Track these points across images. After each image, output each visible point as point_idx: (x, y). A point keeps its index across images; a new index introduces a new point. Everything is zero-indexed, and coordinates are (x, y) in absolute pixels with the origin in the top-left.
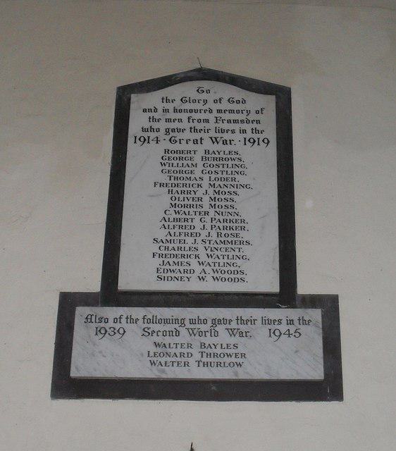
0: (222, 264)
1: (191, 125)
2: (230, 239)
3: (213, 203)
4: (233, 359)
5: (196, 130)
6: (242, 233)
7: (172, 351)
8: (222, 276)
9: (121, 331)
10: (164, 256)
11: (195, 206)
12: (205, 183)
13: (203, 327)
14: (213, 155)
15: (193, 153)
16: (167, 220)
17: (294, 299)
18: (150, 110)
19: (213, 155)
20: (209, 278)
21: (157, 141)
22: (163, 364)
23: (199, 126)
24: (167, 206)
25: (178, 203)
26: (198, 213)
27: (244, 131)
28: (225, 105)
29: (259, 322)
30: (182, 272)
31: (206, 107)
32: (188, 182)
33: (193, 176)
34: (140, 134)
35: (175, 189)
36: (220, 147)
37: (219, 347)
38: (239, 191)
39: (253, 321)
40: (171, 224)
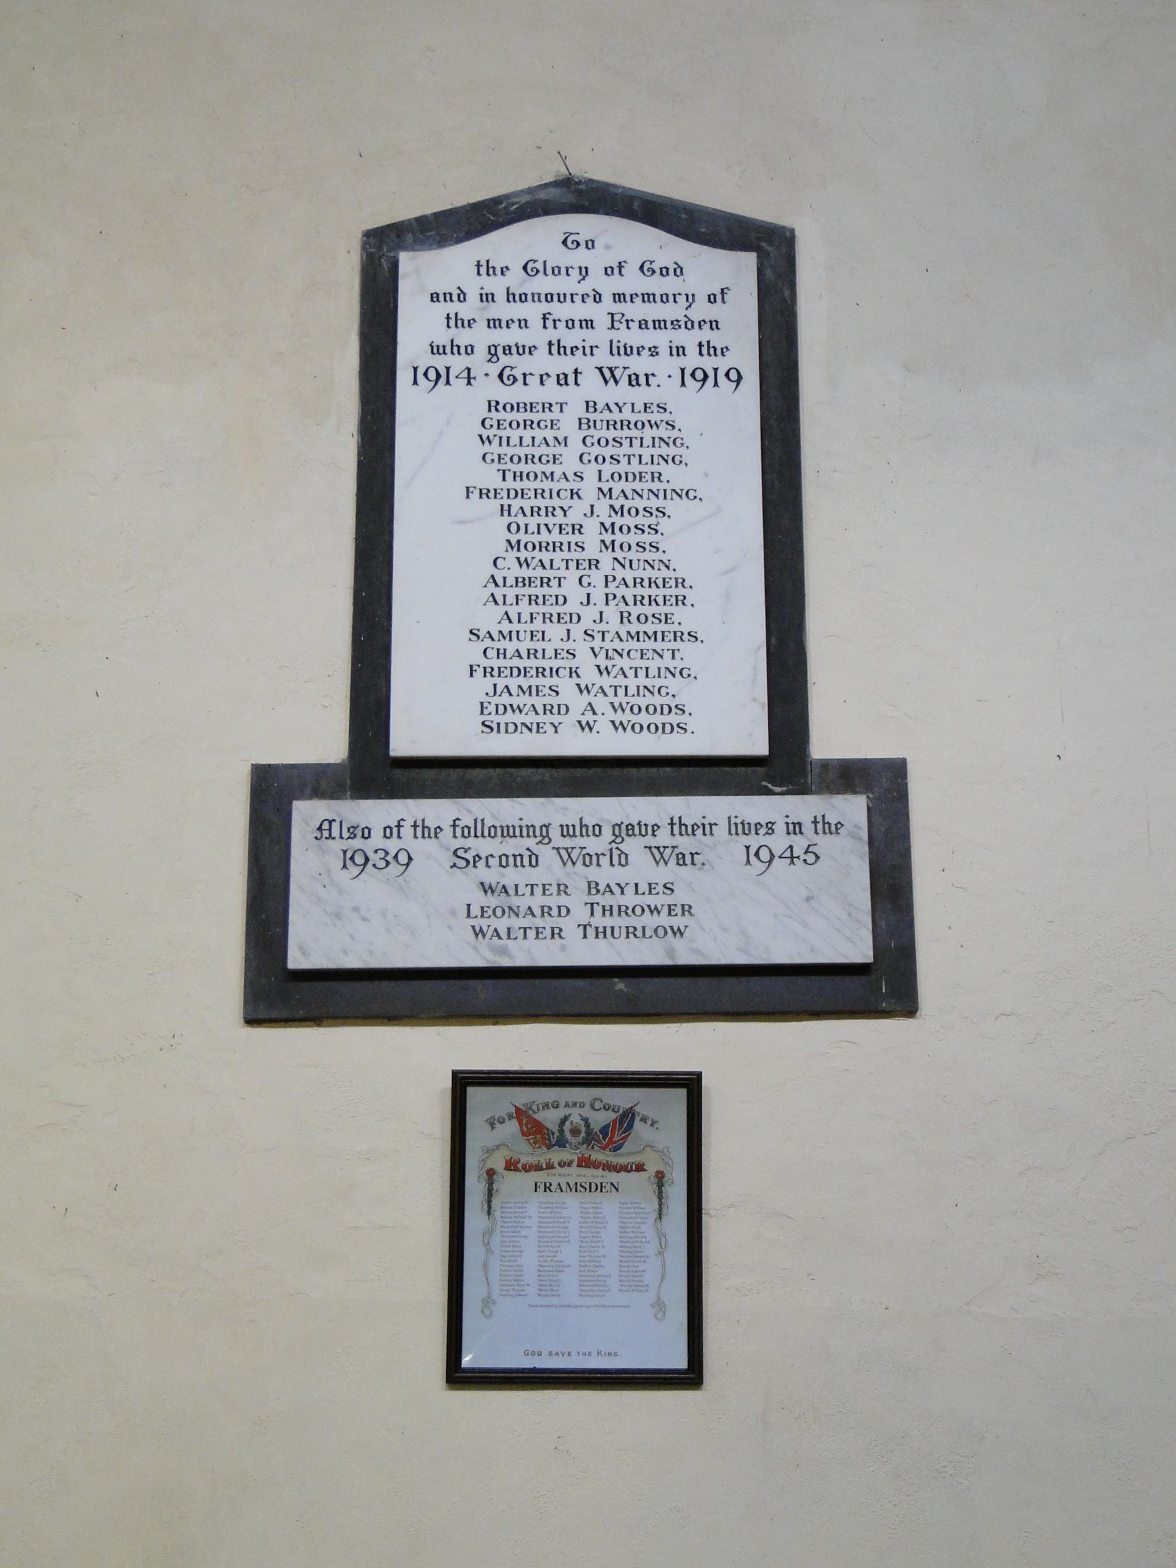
0: (632, 690)
1: (552, 334)
2: (650, 628)
3: (608, 538)
4: (663, 920)
5: (562, 350)
6: (679, 613)
7: (522, 903)
8: (635, 719)
9: (403, 858)
10: (496, 673)
11: (565, 547)
12: (589, 487)
13: (594, 845)
14: (607, 415)
15: (556, 408)
16: (500, 582)
17: (804, 772)
18: (448, 297)
19: (607, 415)
20: (603, 724)
21: (469, 378)
22: (504, 934)
23: (572, 338)
24: (500, 548)
25: (524, 538)
26: (572, 565)
27: (681, 351)
28: (632, 282)
29: (721, 831)
30: (540, 710)
31: (586, 287)
32: (547, 485)
33: (558, 470)
34: (426, 360)
35: (516, 504)
36: (621, 392)
37: (630, 890)
38: (671, 506)
39: (708, 828)
40: (511, 593)
